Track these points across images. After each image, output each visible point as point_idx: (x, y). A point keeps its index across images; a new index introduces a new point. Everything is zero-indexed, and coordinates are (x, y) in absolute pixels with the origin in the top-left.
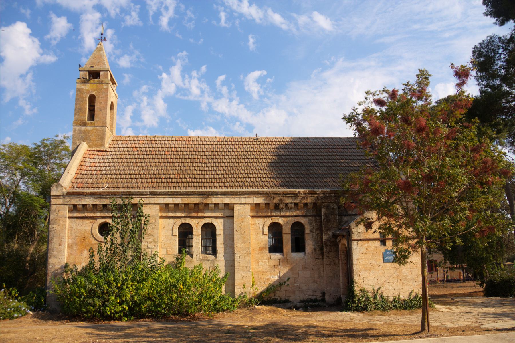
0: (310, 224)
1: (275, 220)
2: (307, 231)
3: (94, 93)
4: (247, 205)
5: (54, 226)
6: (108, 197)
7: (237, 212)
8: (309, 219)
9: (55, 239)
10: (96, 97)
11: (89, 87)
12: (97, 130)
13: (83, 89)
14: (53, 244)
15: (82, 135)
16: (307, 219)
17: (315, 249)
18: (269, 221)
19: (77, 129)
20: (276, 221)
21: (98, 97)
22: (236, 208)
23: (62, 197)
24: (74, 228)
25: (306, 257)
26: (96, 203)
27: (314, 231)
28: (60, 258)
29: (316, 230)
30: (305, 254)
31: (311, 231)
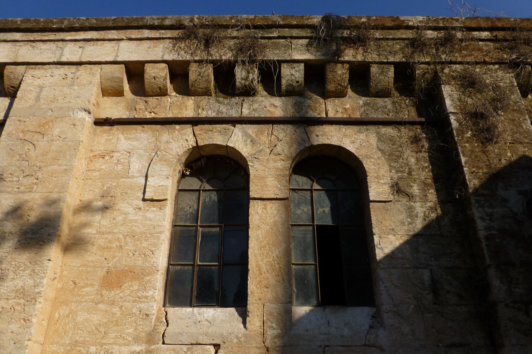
0: (393, 157)
1: (214, 137)
2: (378, 189)
4: (82, 71)
7: (32, 96)
8: (380, 138)
16: (373, 139)
17: (435, 287)
18: (180, 142)
20: (219, 140)
22: (31, 83)
25: (383, 337)
27: (415, 190)
29: (425, 185)
30: (377, 317)
31: (397, 189)
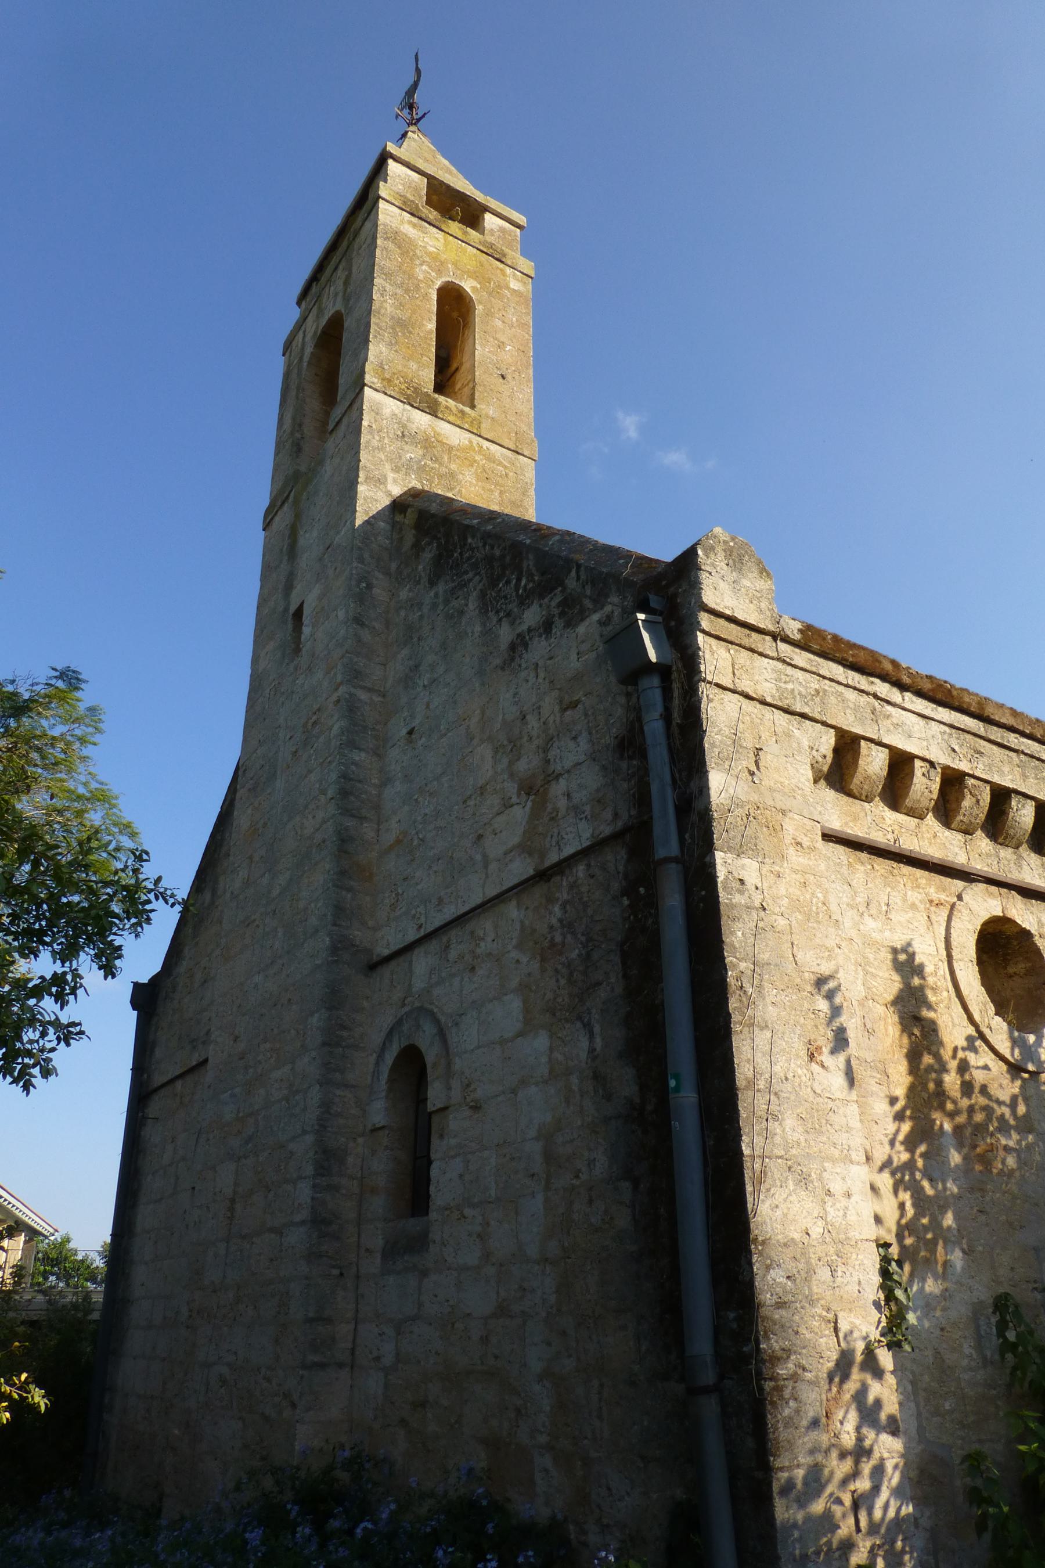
3: (468, 285)
5: (749, 869)
6: (1013, 740)
9: (771, 994)
10: (479, 309)
11: (440, 245)
12: (490, 458)
13: (411, 242)
14: (762, 1038)
15: (412, 453)
19: (386, 412)
21: (489, 314)
23: (766, 644)
24: (848, 923)
26: (964, 766)
28: (837, 1187)
